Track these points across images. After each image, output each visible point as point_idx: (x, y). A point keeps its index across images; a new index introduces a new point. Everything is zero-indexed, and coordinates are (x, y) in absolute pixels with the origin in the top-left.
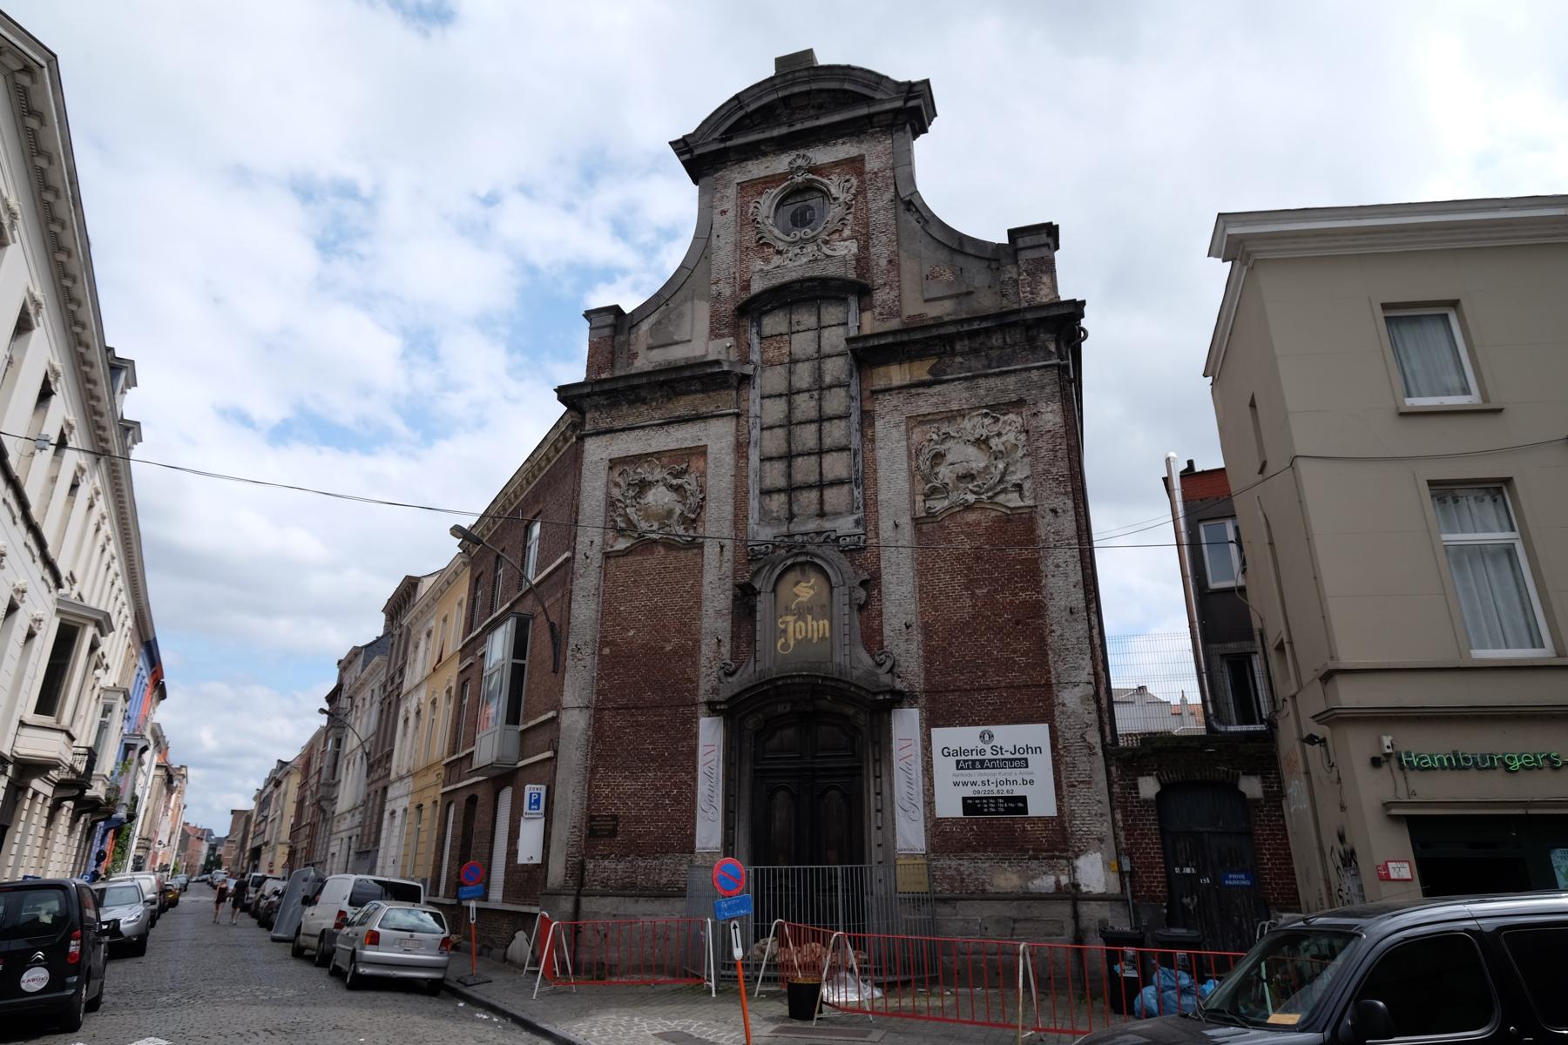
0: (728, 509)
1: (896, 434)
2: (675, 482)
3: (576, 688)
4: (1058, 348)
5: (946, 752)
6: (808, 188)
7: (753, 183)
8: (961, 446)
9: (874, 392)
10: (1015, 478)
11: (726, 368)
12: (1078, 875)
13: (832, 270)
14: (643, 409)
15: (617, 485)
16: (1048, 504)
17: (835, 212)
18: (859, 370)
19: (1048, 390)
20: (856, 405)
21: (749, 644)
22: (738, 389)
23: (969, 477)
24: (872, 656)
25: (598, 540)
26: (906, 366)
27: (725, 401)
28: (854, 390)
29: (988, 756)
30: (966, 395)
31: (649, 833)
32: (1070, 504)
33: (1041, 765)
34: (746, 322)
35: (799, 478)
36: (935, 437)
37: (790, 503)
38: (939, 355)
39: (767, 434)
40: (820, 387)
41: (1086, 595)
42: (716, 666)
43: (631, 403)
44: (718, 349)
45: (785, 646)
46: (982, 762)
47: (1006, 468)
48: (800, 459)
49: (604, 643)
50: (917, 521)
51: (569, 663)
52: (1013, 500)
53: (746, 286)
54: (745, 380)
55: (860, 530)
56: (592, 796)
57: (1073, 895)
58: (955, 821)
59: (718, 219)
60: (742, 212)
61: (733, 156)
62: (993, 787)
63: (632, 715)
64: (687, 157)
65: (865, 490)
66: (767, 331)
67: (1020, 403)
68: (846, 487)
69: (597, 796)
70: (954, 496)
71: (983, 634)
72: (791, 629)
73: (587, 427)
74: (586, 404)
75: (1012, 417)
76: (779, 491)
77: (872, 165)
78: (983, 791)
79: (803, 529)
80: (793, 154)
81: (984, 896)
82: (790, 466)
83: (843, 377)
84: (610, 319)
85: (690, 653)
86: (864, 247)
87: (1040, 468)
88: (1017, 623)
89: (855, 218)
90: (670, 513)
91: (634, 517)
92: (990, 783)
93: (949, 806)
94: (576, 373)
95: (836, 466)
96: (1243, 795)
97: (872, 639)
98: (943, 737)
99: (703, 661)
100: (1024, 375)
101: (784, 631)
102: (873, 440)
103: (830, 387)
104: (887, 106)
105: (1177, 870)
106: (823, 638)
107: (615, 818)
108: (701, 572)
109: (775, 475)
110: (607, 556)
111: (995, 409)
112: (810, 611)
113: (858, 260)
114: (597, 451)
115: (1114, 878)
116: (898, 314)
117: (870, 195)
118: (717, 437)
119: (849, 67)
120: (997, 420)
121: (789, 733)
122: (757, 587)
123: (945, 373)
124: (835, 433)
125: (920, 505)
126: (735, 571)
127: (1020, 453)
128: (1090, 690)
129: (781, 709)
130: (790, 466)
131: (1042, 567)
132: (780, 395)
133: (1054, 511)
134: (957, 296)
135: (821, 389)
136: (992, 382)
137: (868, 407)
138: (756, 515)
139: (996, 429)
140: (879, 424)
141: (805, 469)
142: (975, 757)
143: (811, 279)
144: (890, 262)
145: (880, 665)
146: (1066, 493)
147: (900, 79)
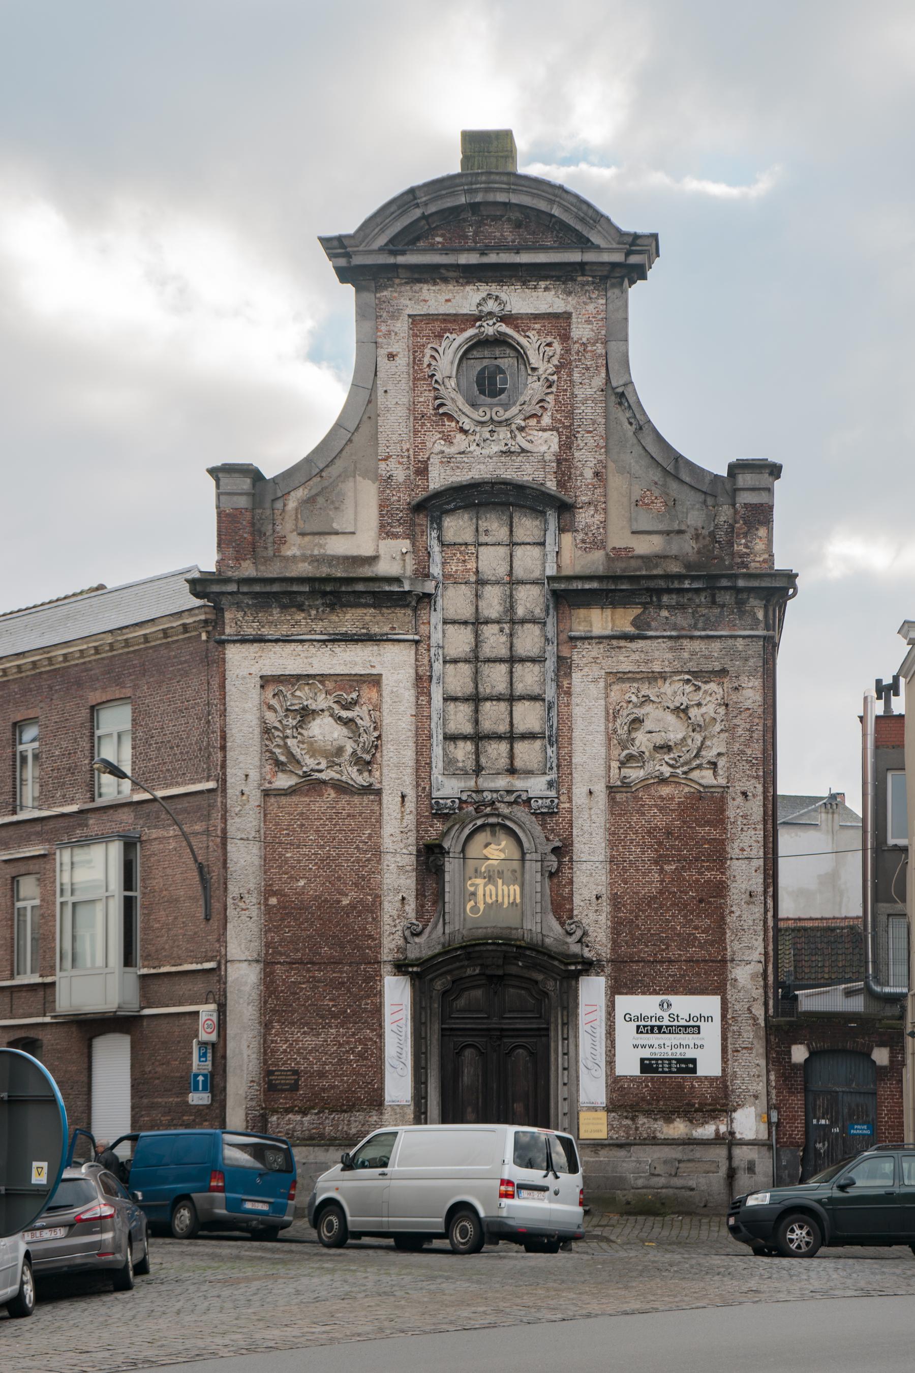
0: (409, 755)
1: (596, 690)
2: (345, 714)
3: (243, 941)
4: (766, 616)
5: (628, 1018)
6: (500, 341)
7: (430, 318)
8: (660, 713)
9: (572, 639)
10: (709, 754)
11: (407, 588)
12: (734, 1125)
13: (525, 472)
14: (300, 616)
15: (271, 708)
16: (739, 787)
17: (534, 388)
18: (556, 608)
19: (751, 662)
20: (551, 649)
21: (435, 903)
22: (415, 610)
23: (667, 748)
24: (562, 924)
25: (254, 775)
26: (608, 612)
27: (398, 620)
28: (551, 630)
29: (666, 1022)
30: (669, 656)
31: (333, 1087)
32: (760, 788)
33: (712, 1032)
34: (421, 519)
35: (487, 726)
36: (634, 699)
37: (477, 754)
38: (645, 605)
39: (450, 668)
40: (512, 621)
41: (765, 879)
42: (401, 924)
43: (284, 607)
44: (392, 559)
45: (475, 909)
46: (660, 1028)
47: (702, 743)
48: (488, 704)
49: (268, 892)
50: (611, 790)
51: (231, 912)
52: (706, 777)
53: (422, 471)
54: (427, 599)
55: (553, 793)
56: (267, 1051)
57: (729, 1141)
58: (632, 1079)
59: (383, 362)
60: (416, 362)
61: (403, 273)
62: (668, 1050)
63: (308, 971)
64: (342, 262)
65: (558, 748)
66: (450, 535)
67: (723, 672)
68: (538, 744)
69: (273, 1051)
70: (650, 767)
71: (668, 910)
72: (480, 892)
73: (228, 630)
74: (224, 601)
75: (713, 686)
76: (465, 738)
77: (580, 331)
78: (658, 1053)
79: (492, 785)
80: (484, 289)
81: (653, 1141)
82: (476, 711)
83: (538, 612)
84: (246, 484)
85: (371, 908)
86: (567, 445)
87: (736, 747)
88: (701, 901)
89: (557, 401)
90: (340, 751)
91: (296, 751)
92: (666, 1047)
93: (628, 1065)
94: (207, 560)
95: (528, 717)
96: (874, 1062)
97: (561, 907)
98: (626, 1003)
99: (386, 919)
100: (730, 642)
101: (474, 894)
102: (569, 693)
103: (523, 622)
104: (606, 258)
105: (815, 1121)
106: (514, 904)
107: (296, 1072)
108: (379, 821)
109: (460, 719)
110: (266, 794)
111: (698, 676)
112: (501, 874)
113: (559, 462)
114: (244, 664)
115: (763, 1127)
116: (602, 545)
117: (576, 376)
118: (394, 665)
119: (561, 188)
120: (699, 688)
121: (478, 993)
122: (446, 845)
123: (649, 628)
124: (528, 678)
125: (614, 772)
126: (419, 824)
127: (718, 727)
128: (760, 968)
129: (469, 972)
130: (476, 711)
131: (728, 849)
132: (465, 623)
133: (744, 794)
134: (668, 533)
135: (513, 622)
136: (697, 645)
137: (565, 653)
138: (440, 765)
139: (697, 697)
140: (576, 676)
141: (493, 716)
142: (653, 1023)
143: (505, 483)
144: (597, 474)
145: (570, 934)
146: (757, 777)
147: (625, 228)
